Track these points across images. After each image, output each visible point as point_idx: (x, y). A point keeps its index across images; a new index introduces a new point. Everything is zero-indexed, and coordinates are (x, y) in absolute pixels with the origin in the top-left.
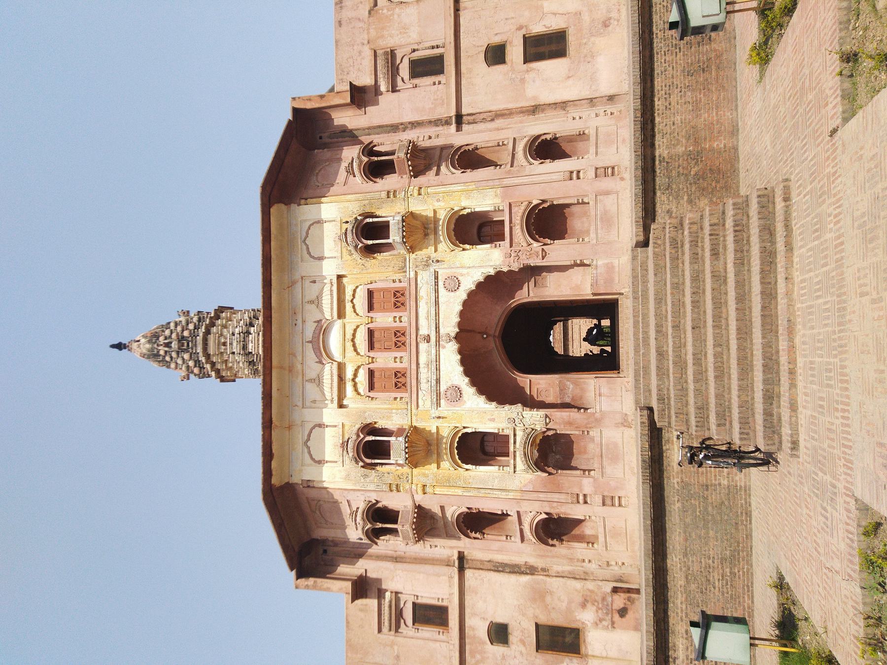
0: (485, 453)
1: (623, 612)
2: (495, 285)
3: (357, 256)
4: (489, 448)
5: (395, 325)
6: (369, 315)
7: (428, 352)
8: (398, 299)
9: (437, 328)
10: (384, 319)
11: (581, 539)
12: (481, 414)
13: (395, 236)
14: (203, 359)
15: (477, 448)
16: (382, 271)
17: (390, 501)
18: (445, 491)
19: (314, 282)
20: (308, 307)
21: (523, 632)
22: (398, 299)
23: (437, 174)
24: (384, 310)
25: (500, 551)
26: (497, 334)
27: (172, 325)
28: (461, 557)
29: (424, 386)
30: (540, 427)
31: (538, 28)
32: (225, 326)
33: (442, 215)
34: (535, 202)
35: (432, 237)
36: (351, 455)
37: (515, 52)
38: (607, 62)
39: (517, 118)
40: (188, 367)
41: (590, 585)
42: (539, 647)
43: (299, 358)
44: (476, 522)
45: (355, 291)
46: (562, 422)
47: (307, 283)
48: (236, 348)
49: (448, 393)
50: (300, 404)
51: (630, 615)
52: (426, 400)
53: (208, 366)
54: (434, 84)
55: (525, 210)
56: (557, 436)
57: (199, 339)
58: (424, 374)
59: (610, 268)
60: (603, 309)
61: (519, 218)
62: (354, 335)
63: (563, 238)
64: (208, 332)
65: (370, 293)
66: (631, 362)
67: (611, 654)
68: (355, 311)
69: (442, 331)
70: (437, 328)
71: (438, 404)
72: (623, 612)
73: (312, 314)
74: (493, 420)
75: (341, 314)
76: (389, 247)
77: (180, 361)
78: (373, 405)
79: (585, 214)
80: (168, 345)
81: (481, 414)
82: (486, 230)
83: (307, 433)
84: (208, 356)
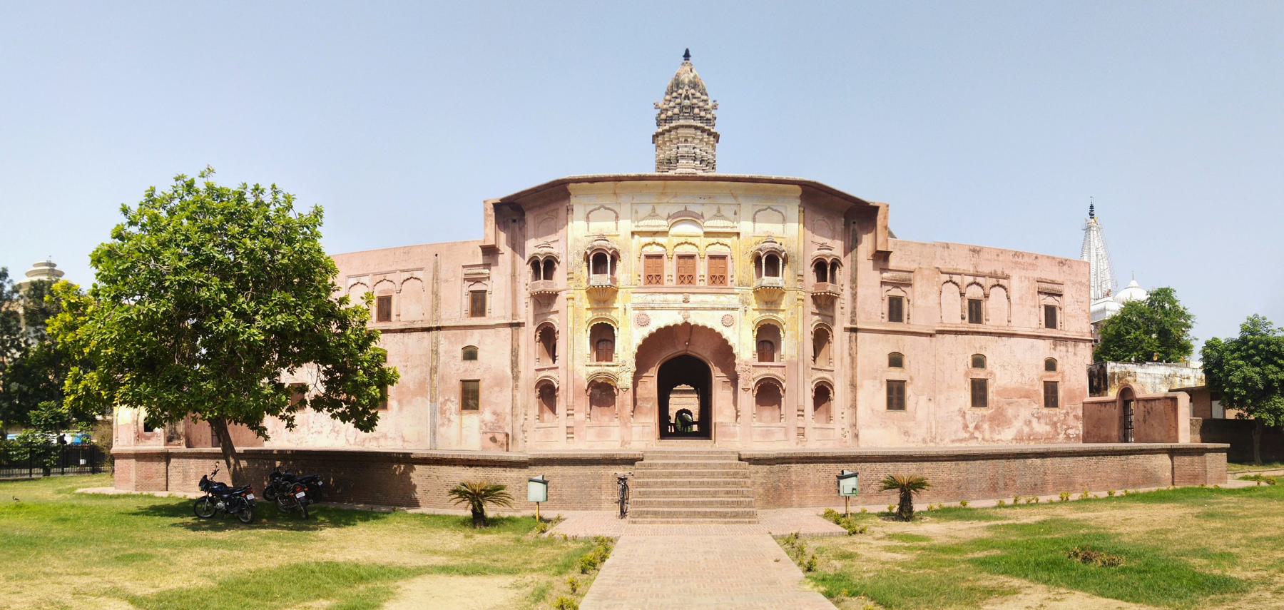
1: (493, 440)
2: (725, 353)
3: (754, 249)
7: (675, 302)
8: (718, 279)
9: (694, 309)
10: (702, 268)
11: (541, 411)
12: (628, 341)
14: (674, 124)
15: (603, 337)
16: (740, 267)
18: (570, 314)
21: (472, 371)
22: (718, 279)
23: (813, 313)
24: (710, 267)
25: (527, 354)
27: (704, 97)
28: (519, 325)
29: (650, 298)
30: (620, 384)
32: (701, 140)
33: (781, 316)
34: (784, 385)
38: (881, 433)
39: (849, 372)
41: (508, 418)
42: (463, 381)
44: (548, 337)
46: (624, 399)
47: (735, 208)
48: (682, 150)
51: (492, 444)
52: (639, 299)
53: (667, 127)
56: (613, 396)
57: (692, 122)
58: (659, 298)
59: (733, 435)
60: (705, 430)
63: (757, 403)
64: (696, 128)
65: (724, 257)
66: (670, 449)
67: (464, 432)
70: (694, 309)
71: (635, 309)
72: (493, 440)
73: (708, 211)
75: (707, 234)
76: (759, 275)
77: (672, 104)
78: (634, 258)
79: (773, 419)
80: (687, 97)
81: (628, 341)
82: (768, 346)
84: (676, 128)
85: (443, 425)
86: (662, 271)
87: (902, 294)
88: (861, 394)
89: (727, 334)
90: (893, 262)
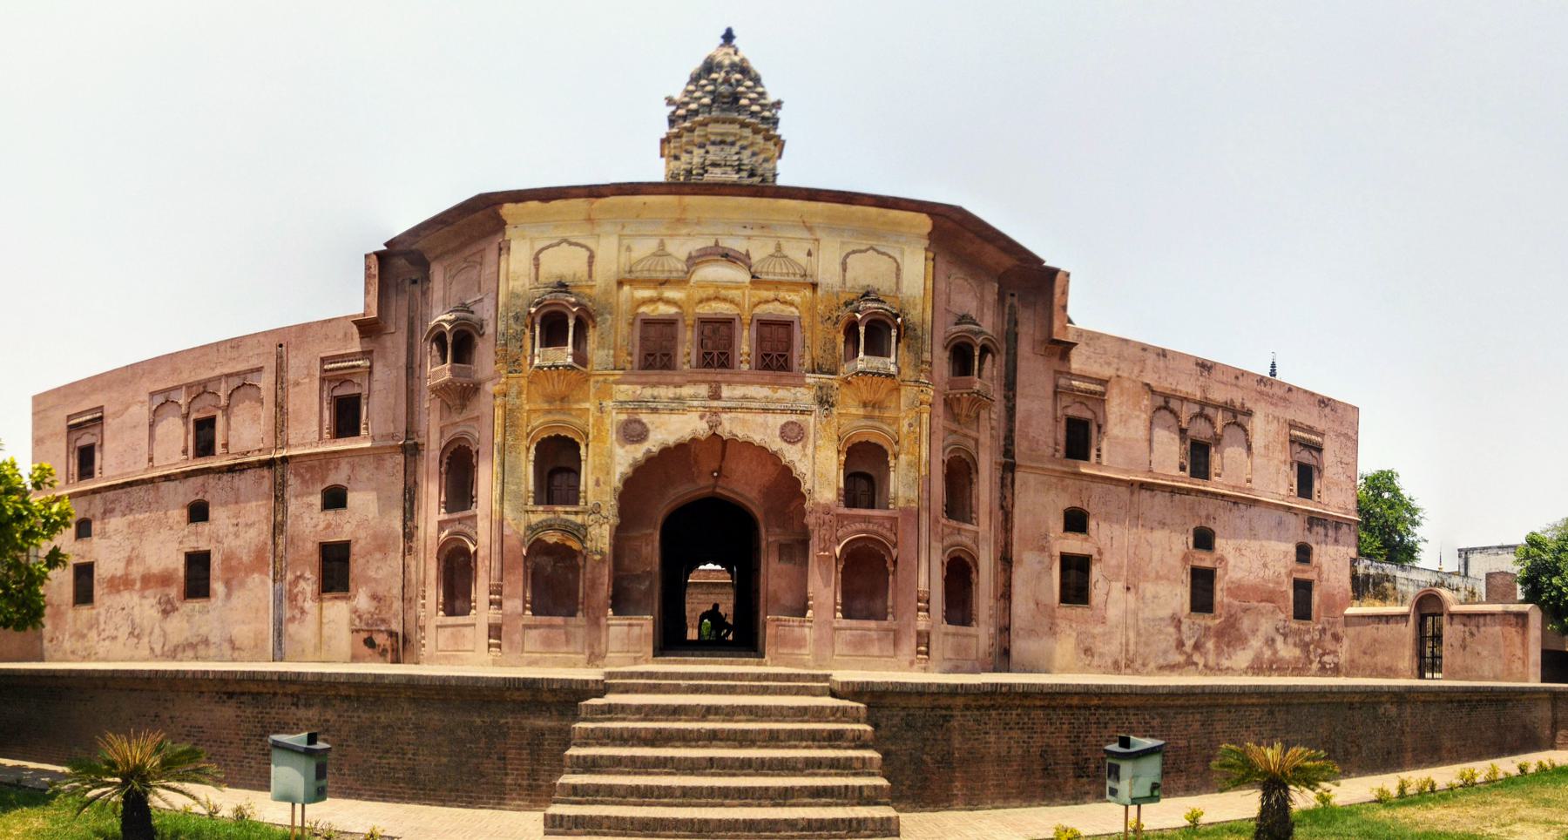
0: (552, 474)
4: (558, 480)
7: (695, 397)
12: (607, 466)
15: (558, 464)
29: (648, 392)
40: (687, 104)
49: (637, 426)
50: (627, 231)
58: (665, 392)
78: (623, 328)
81: (607, 466)
82: (862, 485)
85: (293, 619)
86: (674, 347)
87: (1087, 415)
88: (1020, 576)
89: (791, 454)
90: (1077, 362)
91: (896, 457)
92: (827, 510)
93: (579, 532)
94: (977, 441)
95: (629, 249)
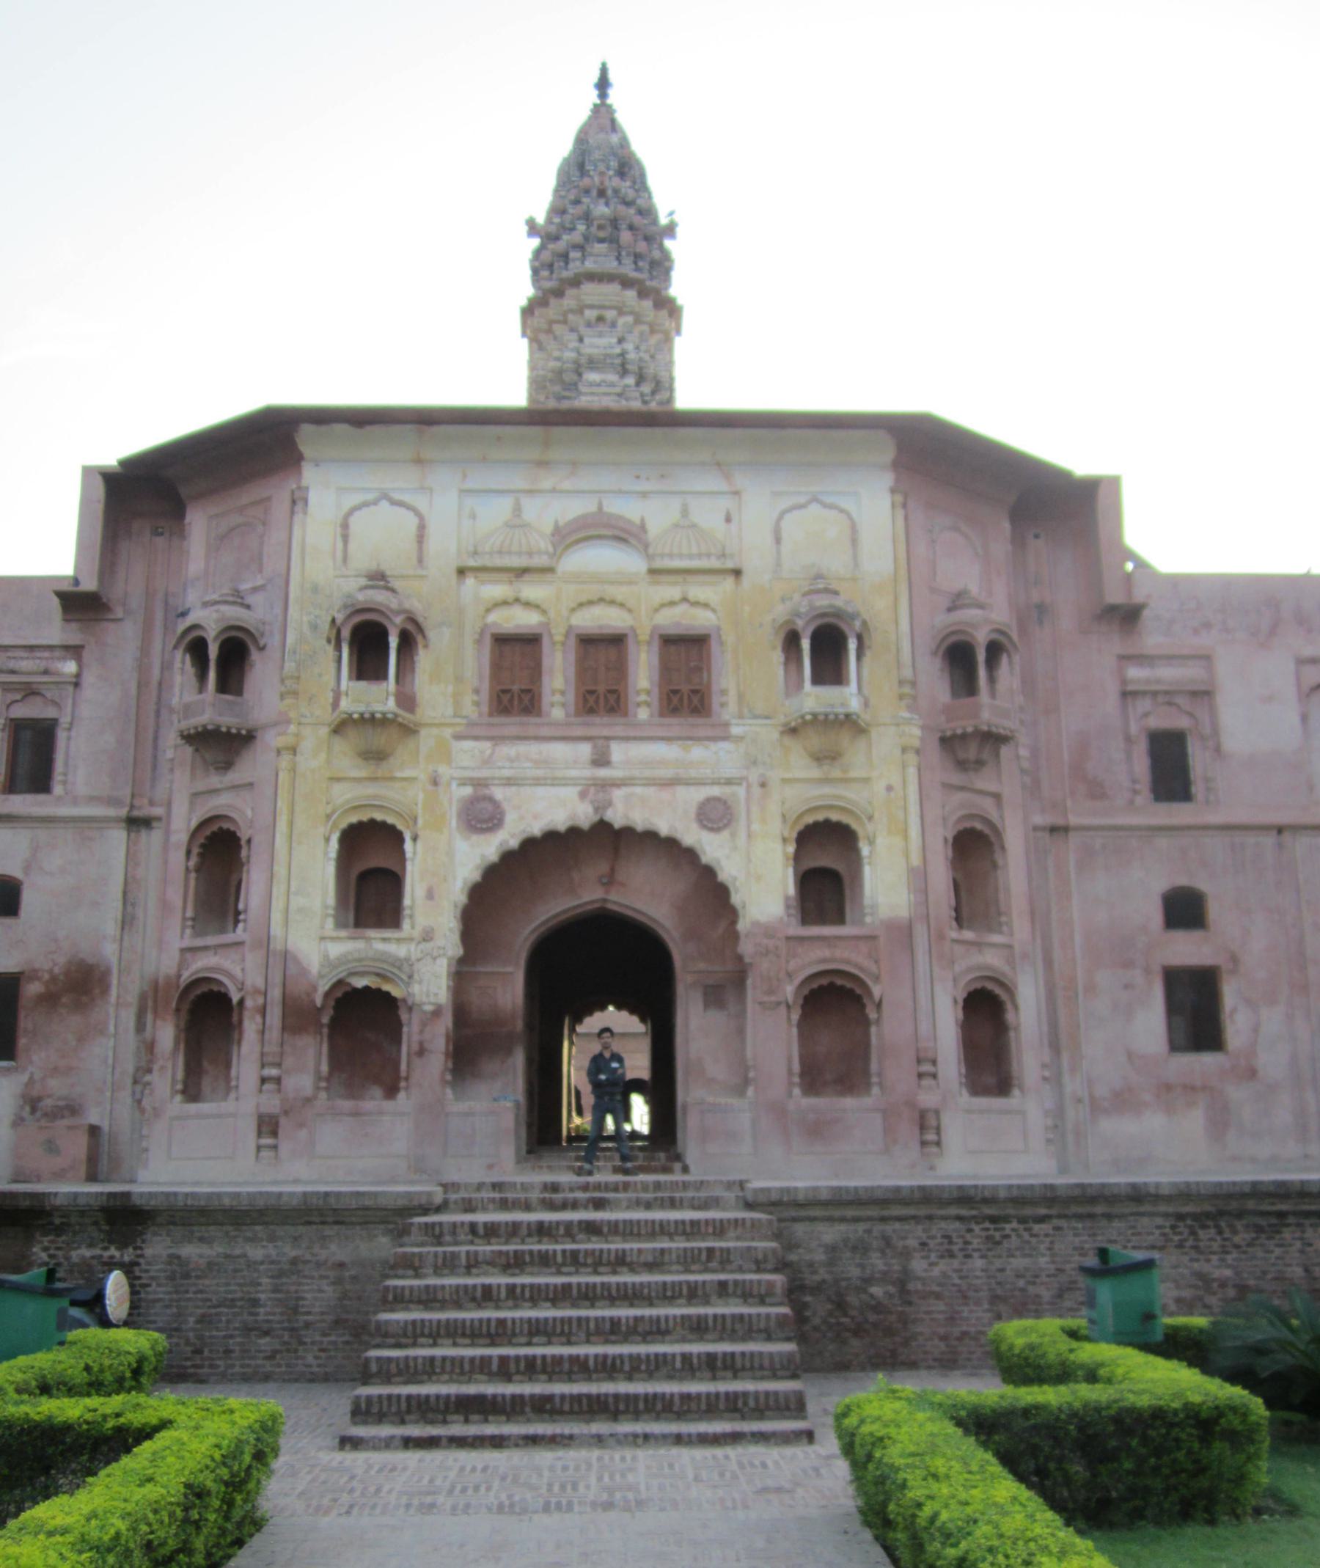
3: (780, 612)
5: (631, 690)
6: (656, 637)
10: (643, 672)
12: (441, 871)
13: (814, 698)
17: (262, 676)
19: (728, 519)
20: (675, 505)
24: (666, 669)
26: (610, 906)
31: (1230, 995)
34: (876, 991)
35: (815, 773)
36: (361, 597)
37: (1187, 950)
43: (566, 485)
45: (706, 605)
47: (725, 503)
54: (1134, 781)
55: (861, 969)
61: (846, 955)
62: (612, 602)
68: (663, 605)
69: (618, 794)
74: (430, 895)
76: (794, 686)
81: (441, 871)
83: (406, 498)
91: (871, 842)
92: (768, 931)
93: (405, 968)
94: (997, 797)
95: (473, 516)
